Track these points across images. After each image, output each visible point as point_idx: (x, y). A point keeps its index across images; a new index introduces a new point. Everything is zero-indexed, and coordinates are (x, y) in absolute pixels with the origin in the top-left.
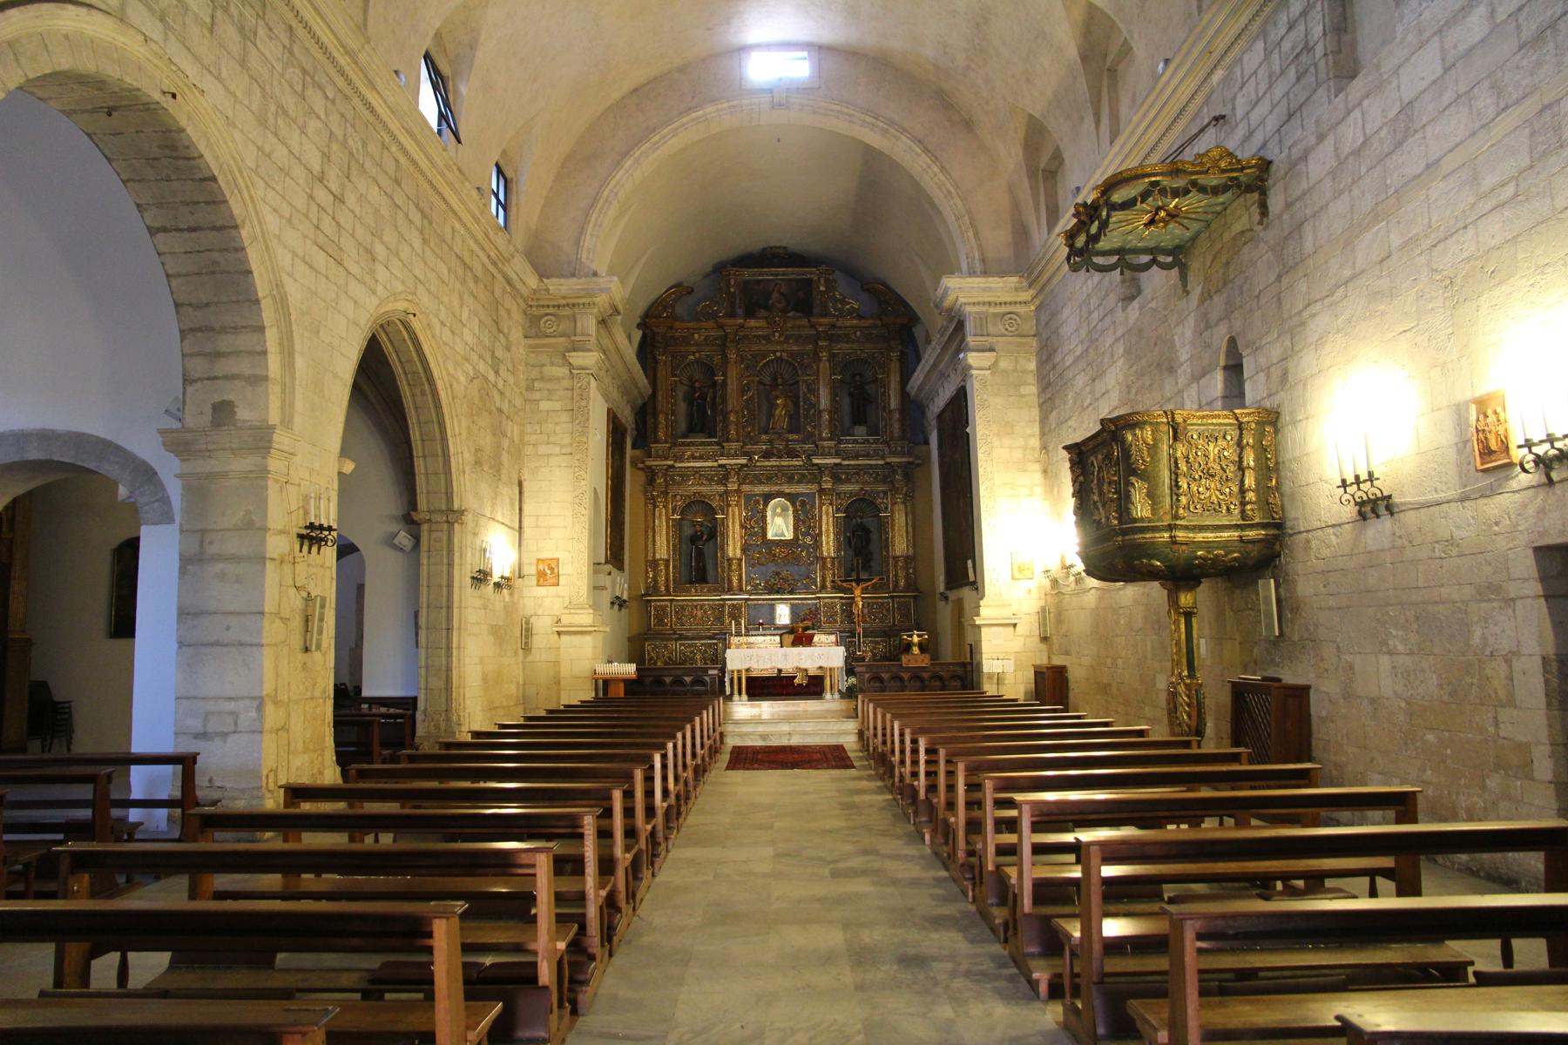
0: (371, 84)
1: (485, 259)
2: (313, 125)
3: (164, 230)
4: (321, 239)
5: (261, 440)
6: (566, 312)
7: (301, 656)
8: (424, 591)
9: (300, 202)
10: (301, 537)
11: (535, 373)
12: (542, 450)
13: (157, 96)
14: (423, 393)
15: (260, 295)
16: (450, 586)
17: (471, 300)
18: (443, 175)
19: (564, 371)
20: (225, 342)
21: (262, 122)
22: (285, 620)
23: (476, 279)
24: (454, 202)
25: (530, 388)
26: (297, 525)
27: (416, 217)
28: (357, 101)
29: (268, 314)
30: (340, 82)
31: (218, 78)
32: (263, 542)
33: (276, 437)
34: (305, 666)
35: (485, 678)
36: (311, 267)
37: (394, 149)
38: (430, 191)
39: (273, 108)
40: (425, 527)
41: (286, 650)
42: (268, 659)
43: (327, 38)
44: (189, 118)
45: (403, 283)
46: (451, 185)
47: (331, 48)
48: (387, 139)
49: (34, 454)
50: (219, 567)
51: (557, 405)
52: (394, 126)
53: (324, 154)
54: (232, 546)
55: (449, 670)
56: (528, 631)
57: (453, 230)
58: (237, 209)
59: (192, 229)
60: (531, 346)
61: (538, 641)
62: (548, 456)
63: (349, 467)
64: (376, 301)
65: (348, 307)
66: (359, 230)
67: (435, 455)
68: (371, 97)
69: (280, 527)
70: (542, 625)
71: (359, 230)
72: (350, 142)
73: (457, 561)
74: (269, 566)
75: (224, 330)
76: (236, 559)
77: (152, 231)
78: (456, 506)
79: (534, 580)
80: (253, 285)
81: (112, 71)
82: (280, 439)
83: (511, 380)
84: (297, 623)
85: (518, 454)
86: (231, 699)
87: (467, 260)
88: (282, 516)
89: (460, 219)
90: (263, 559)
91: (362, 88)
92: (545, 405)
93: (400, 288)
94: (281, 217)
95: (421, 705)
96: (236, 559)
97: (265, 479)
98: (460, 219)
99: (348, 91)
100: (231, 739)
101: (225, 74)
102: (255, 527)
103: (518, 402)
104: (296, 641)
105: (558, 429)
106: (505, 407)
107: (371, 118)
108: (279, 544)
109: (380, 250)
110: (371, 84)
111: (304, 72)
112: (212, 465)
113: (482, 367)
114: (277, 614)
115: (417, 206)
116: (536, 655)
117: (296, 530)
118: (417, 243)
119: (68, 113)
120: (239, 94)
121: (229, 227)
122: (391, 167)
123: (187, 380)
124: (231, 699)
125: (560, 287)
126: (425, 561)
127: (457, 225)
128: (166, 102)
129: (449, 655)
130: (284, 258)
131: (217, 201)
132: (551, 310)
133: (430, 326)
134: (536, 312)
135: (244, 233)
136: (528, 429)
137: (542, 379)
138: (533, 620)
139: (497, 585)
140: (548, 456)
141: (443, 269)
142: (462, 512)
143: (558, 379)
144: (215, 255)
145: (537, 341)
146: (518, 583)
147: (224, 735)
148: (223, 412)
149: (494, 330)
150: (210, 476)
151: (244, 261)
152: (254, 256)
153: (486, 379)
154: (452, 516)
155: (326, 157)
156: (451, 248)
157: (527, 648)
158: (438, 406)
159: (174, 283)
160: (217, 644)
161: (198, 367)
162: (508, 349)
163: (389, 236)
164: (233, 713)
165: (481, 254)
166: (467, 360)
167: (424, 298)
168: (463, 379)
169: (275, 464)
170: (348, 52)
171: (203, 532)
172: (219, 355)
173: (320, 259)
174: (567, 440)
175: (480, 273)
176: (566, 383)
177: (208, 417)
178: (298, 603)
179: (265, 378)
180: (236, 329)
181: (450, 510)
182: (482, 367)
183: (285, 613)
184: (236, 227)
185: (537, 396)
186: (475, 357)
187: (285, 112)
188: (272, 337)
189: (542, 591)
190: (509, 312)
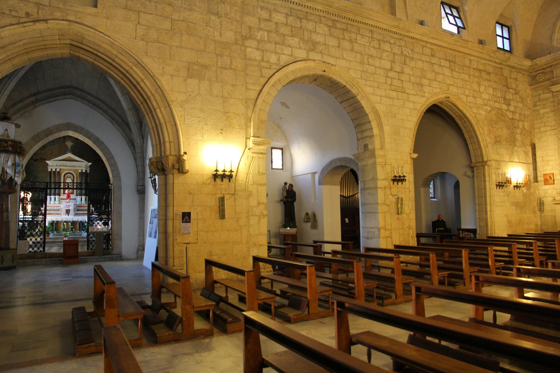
0: (409, 31)
1: (494, 64)
2: (385, 55)
3: (342, 102)
4: (393, 88)
5: (373, 155)
6: (549, 70)
7: (396, 216)
8: (476, 191)
9: (382, 80)
10: (394, 180)
11: (537, 99)
12: (542, 129)
13: (321, 73)
14: (465, 122)
15: (367, 112)
16: (485, 189)
17: (486, 83)
18: (456, 45)
19: (550, 95)
20: (364, 127)
21: (362, 63)
23: (489, 73)
25: (535, 106)
26: (391, 176)
27: (447, 64)
29: (371, 117)
30: (397, 36)
31: (343, 58)
32: (377, 183)
33: (376, 153)
34: (398, 219)
35: (509, 222)
36: (389, 98)
37: (428, 45)
38: (452, 52)
39: (366, 57)
40: (475, 168)
41: (389, 214)
42: (380, 217)
43: (385, 27)
44: (333, 74)
45: (440, 88)
46: (462, 46)
48: (424, 44)
49: (338, 164)
50: (368, 191)
51: (548, 110)
52: (425, 39)
53: (391, 61)
54: (370, 185)
55: (487, 219)
56: (541, 204)
57: (470, 60)
58: (354, 91)
59: (347, 100)
60: (534, 89)
61: (547, 207)
62: (545, 131)
63: (415, 156)
64: (424, 99)
65: (411, 105)
66: (413, 79)
67: (475, 142)
68: (411, 35)
69: (383, 178)
70: (548, 201)
71: (413, 79)
72: (405, 52)
73: (487, 179)
74: (379, 190)
75: (362, 124)
76: (371, 188)
77: (341, 103)
78: (485, 159)
79: (543, 183)
80: (364, 110)
81: (306, 73)
82: (377, 152)
83: (520, 105)
84: (394, 206)
85: (530, 133)
86: (373, 228)
87: (481, 67)
88: (383, 175)
89: (473, 56)
90: (377, 188)
91: (407, 34)
92: (542, 111)
93: (438, 90)
94: (373, 87)
95: (478, 232)
96: (371, 188)
97: (376, 165)
98: (473, 56)
99: (401, 37)
100: (374, 239)
101: (345, 56)
102: (375, 179)
103: (527, 113)
104: (394, 211)
105: (549, 119)
106: (517, 117)
107: (414, 41)
108: (380, 184)
109: (425, 82)
110: (409, 31)
111: (379, 40)
112: (364, 163)
113: (497, 105)
114: (385, 204)
115: (446, 60)
116: (546, 213)
117: (390, 178)
118: (447, 72)
119: (310, 83)
120: (351, 59)
121: (354, 97)
122: (428, 51)
123: (358, 140)
124: (373, 228)
125: (541, 61)
126: (476, 181)
127: (472, 58)
128: (324, 73)
129: (486, 214)
130: (374, 99)
131: (349, 91)
132: (541, 71)
133: (459, 99)
134: (534, 74)
135: (359, 98)
136: (536, 122)
137: (540, 100)
138: (544, 199)
139: (517, 187)
140: (545, 131)
141: (466, 77)
142: (486, 162)
143: (547, 99)
144: (355, 105)
145: (536, 86)
146: (533, 185)
147: (372, 238)
148: (366, 146)
149: (505, 89)
150: (364, 166)
151: (361, 105)
152: (363, 103)
153: (500, 109)
154: (483, 163)
155: (393, 62)
156: (469, 68)
157: (541, 210)
158: (471, 125)
159: (350, 114)
160: (369, 213)
161: (360, 136)
162: (517, 93)
163: (430, 75)
164: (373, 232)
165: (490, 63)
166: (486, 105)
167: (454, 90)
168: (483, 113)
169: (378, 160)
171: (364, 181)
172: (363, 131)
173: (394, 94)
174: (553, 124)
175: (491, 70)
176: (551, 100)
177: (363, 149)
178: (394, 200)
179: (373, 136)
180: (365, 123)
181: (483, 161)
182: (497, 105)
183: (388, 202)
184: (355, 96)
185: (538, 108)
186: (491, 103)
187: (372, 56)
188: (374, 124)
189: (547, 187)
190: (516, 79)
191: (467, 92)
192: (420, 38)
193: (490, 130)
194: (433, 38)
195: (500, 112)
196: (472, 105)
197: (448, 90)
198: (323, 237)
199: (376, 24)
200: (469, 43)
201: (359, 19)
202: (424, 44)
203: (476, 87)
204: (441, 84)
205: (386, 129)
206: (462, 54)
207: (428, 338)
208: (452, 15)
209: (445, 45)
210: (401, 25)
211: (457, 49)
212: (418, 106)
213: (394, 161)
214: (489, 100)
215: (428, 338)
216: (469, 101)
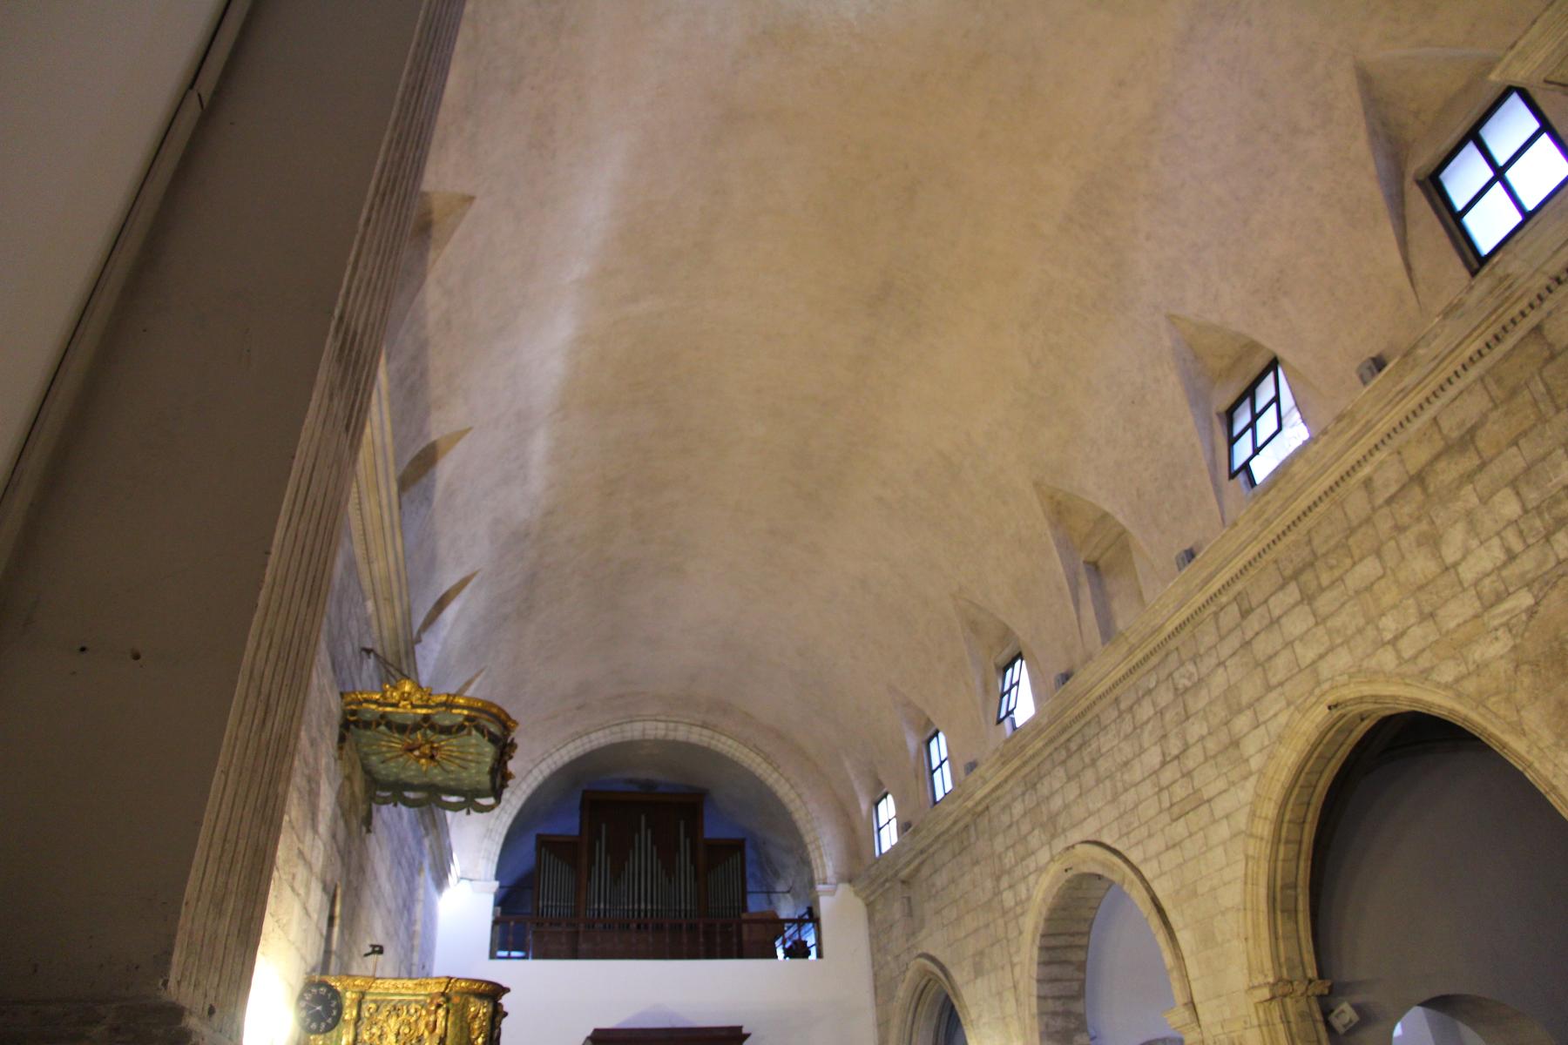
0: (1156, 630)
4: (1176, 810)
18: (1269, 522)
28: (1172, 644)
30: (1154, 660)
37: (1224, 599)
43: (1123, 669)
47: (1130, 665)
48: (1213, 608)
52: (1200, 599)
68: (1170, 628)
91: (1164, 634)
128: (1070, 874)
170: (1131, 651)
191: (1389, 625)
192: (1190, 611)
196: (1424, 662)
197: (1318, 683)
199: (1108, 682)
200: (1295, 469)
201: (1084, 703)
202: (1213, 608)
203: (1421, 565)
204: (1288, 687)
205: (1184, 937)
206: (1322, 508)
208: (1252, 425)
210: (1133, 640)
211: (1298, 512)
212: (1241, 820)
213: (1219, 1030)
214: (1511, 557)
216: (1407, 654)
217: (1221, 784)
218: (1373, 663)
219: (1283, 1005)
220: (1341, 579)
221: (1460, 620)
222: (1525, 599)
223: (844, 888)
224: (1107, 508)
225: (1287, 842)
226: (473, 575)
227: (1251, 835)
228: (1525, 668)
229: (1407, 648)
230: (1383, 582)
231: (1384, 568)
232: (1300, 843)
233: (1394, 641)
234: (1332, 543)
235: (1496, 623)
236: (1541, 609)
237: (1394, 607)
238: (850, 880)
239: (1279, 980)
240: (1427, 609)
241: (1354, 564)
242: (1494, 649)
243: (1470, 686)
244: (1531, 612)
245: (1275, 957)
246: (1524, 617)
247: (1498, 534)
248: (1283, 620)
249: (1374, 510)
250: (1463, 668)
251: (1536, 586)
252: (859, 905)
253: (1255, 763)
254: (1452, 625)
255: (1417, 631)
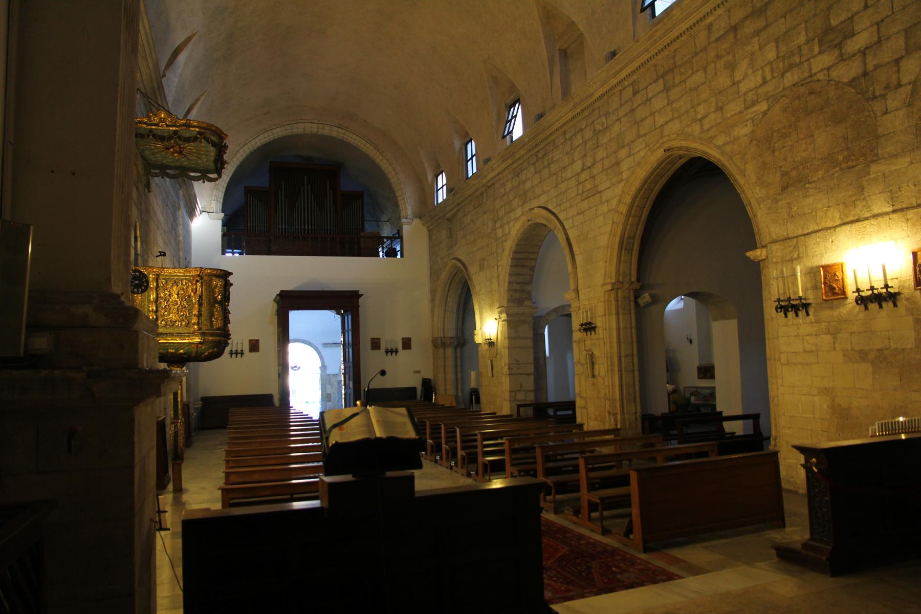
7: (591, 379)
22: (582, 365)
24: (684, 26)
28: (596, 105)
30: (586, 113)
34: (593, 384)
37: (626, 83)
43: (570, 116)
52: (614, 81)
68: (596, 96)
91: (592, 100)
128: (530, 223)
170: (575, 106)
191: (701, 110)
192: (608, 88)
193: (764, 164)
194: (619, 72)
195: (802, 90)
196: (711, 133)
197: (662, 138)
198: (547, 398)
199: (561, 122)
200: (674, 12)
201: (548, 132)
202: (620, 88)
203: (723, 80)
205: (579, 258)
206: (684, 37)
207: (389, 474)
209: (644, 58)
210: (577, 100)
211: (671, 39)
212: (614, 203)
214: (765, 82)
215: (389, 474)
216: (705, 128)
217: (607, 184)
218: (689, 130)
219: (617, 293)
220: (684, 81)
221: (733, 113)
222: (763, 107)
223: (417, 221)
224: (574, 19)
225: (634, 216)
226: (194, 35)
227: (617, 212)
228: (754, 142)
229: (707, 124)
230: (703, 86)
231: (706, 78)
232: (640, 217)
233: (701, 120)
234: (685, 59)
235: (748, 117)
236: (769, 113)
237: (706, 101)
238: (420, 216)
239: (618, 281)
240: (720, 105)
241: (693, 74)
242: (743, 131)
243: (728, 149)
244: (765, 114)
245: (618, 270)
246: (761, 116)
247: (762, 68)
248: (653, 100)
249: (709, 43)
250: (728, 139)
251: (771, 100)
252: (424, 230)
253: (625, 176)
254: (729, 115)
255: (713, 116)
